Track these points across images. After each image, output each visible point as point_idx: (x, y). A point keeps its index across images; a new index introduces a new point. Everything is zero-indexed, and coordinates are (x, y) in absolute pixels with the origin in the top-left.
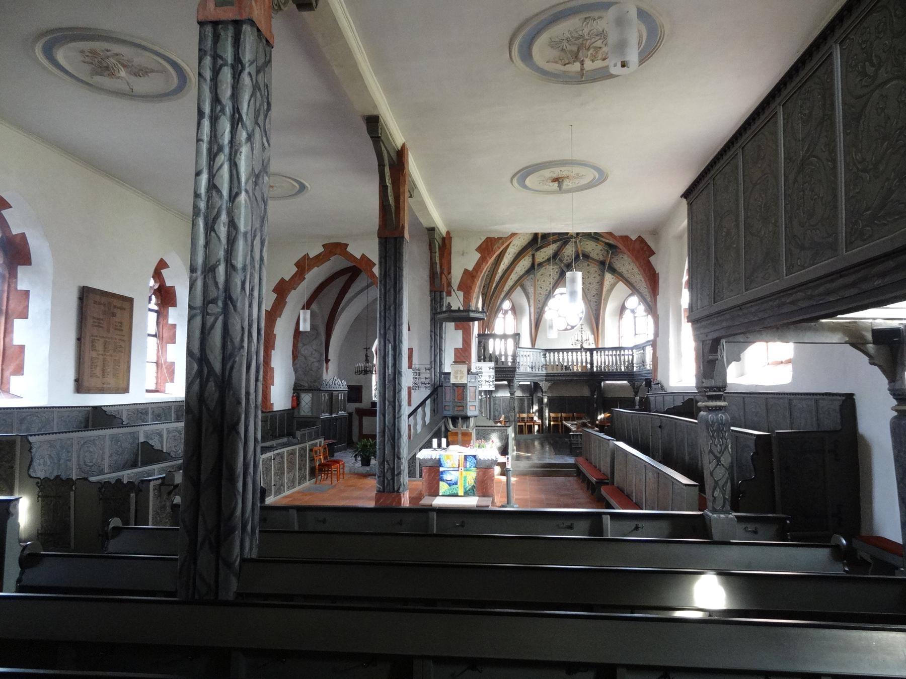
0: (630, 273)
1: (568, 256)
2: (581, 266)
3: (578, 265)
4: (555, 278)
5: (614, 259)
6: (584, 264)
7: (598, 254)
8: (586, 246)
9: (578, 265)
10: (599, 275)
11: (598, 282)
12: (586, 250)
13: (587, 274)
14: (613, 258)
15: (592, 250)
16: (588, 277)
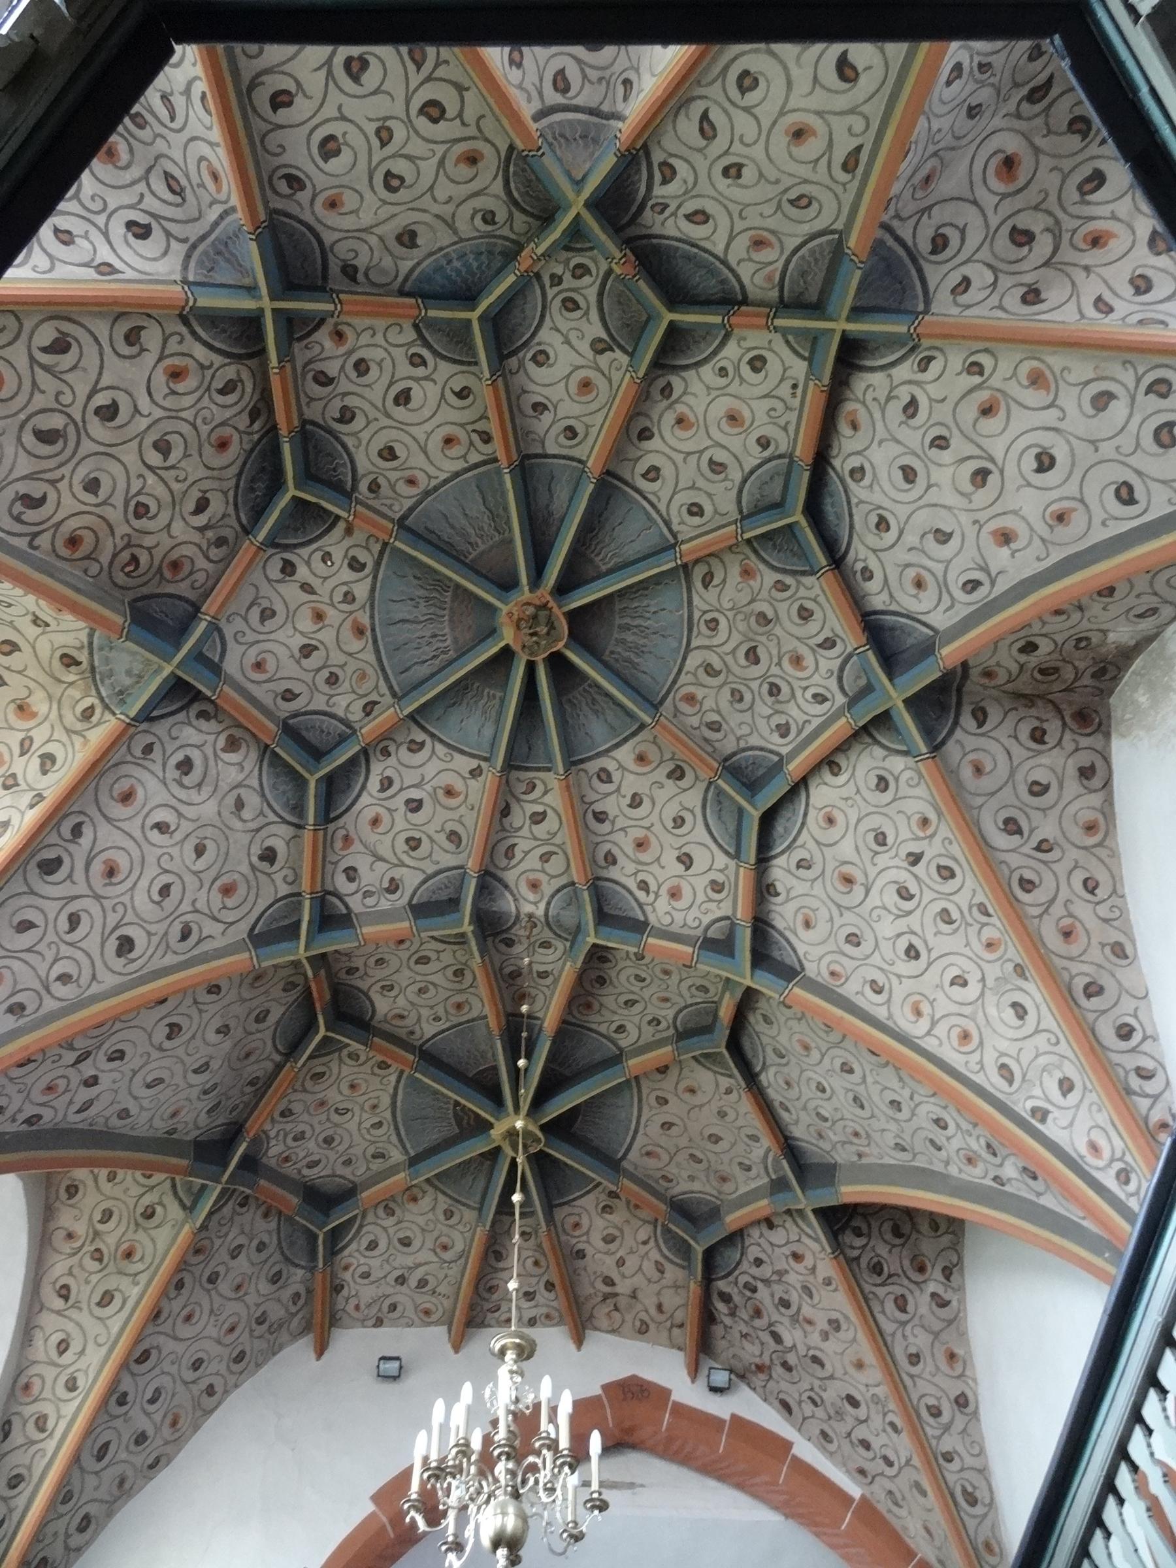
0: (81, 430)
1: (570, 305)
2: (467, 209)
3: (489, 217)
4: (688, 126)
5: (243, 421)
6: (445, 238)
7: (362, 367)
8: (454, 415)
9: (489, 217)
10: (295, 182)
11: (281, 100)
12: (445, 369)
13: (400, 167)
14: (254, 415)
15: (403, 398)
16: (384, 136)
